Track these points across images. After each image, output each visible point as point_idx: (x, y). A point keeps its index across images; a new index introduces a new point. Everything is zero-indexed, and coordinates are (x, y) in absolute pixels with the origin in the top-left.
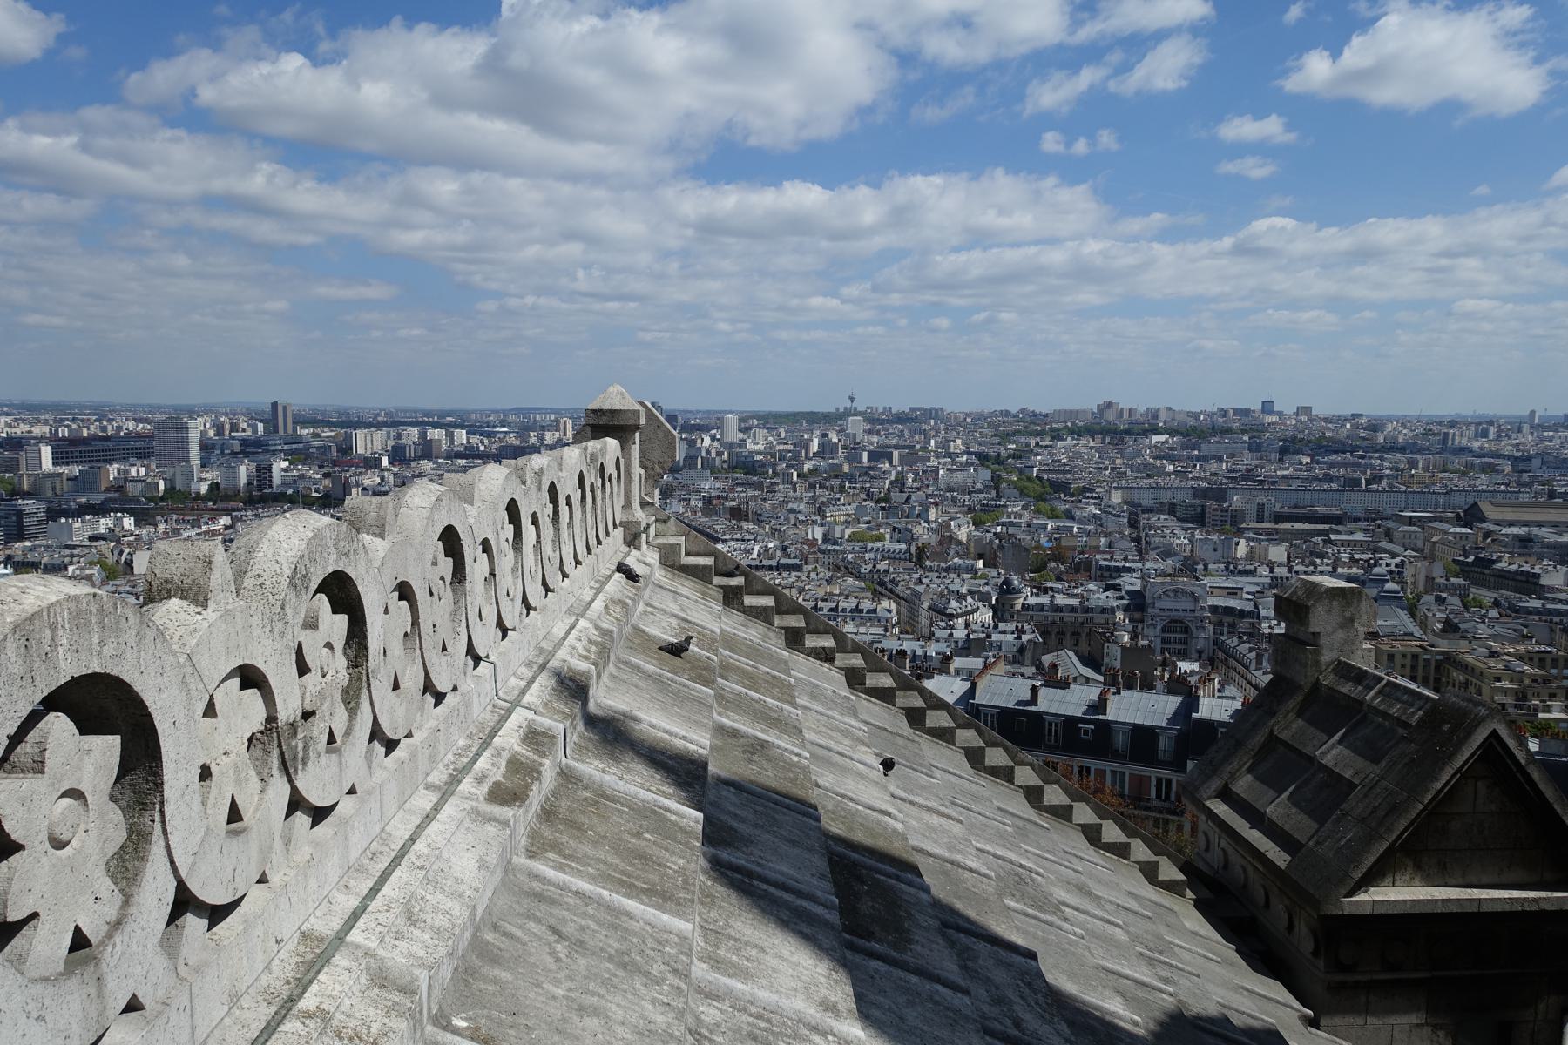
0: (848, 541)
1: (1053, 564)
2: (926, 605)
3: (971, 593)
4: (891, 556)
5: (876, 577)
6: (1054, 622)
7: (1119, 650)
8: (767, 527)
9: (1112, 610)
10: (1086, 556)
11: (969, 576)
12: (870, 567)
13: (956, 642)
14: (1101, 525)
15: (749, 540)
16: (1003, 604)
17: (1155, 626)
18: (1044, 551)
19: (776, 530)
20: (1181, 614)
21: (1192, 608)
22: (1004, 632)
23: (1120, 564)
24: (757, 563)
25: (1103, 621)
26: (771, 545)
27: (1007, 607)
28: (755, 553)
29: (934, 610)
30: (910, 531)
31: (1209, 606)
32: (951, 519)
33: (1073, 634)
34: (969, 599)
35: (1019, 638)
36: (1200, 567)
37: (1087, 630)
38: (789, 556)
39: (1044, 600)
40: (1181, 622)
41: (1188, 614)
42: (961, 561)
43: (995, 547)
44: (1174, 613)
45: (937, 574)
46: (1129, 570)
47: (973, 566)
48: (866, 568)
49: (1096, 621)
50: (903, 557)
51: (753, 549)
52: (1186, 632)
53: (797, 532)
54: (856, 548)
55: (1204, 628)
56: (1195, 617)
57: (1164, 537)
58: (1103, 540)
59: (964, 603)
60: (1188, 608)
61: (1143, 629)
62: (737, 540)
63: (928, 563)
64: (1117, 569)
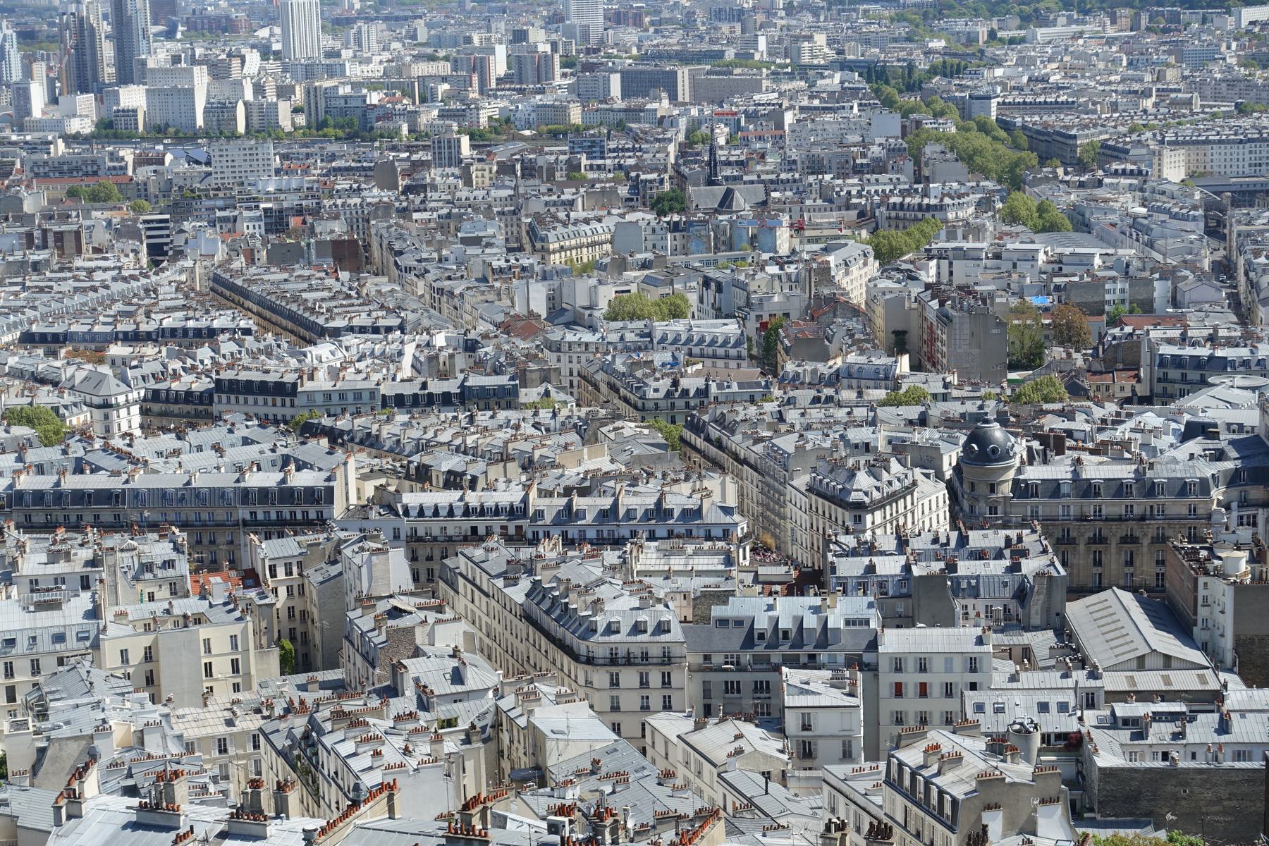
0: (612, 316)
1: (1057, 352)
2: (802, 481)
3: (899, 448)
5: (680, 403)
7: (1230, 591)
8: (421, 284)
10: (1128, 329)
11: (881, 394)
12: (665, 384)
13: (882, 585)
14: (1151, 245)
15: (389, 330)
19: (441, 291)
22: (979, 555)
23: (1204, 352)
24: (409, 390)
25: (1185, 511)
26: (440, 340)
27: (982, 489)
28: (407, 361)
29: (819, 494)
30: (743, 287)
32: (826, 250)
33: (1124, 540)
34: (895, 466)
35: (1015, 568)
37: (1152, 532)
38: (478, 366)
39: (1059, 470)
42: (863, 359)
43: (932, 317)
45: (813, 393)
46: (1222, 366)
50: (733, 352)
51: (400, 354)
53: (491, 297)
54: (630, 337)
59: (885, 476)
62: (362, 330)
64: (1197, 362)
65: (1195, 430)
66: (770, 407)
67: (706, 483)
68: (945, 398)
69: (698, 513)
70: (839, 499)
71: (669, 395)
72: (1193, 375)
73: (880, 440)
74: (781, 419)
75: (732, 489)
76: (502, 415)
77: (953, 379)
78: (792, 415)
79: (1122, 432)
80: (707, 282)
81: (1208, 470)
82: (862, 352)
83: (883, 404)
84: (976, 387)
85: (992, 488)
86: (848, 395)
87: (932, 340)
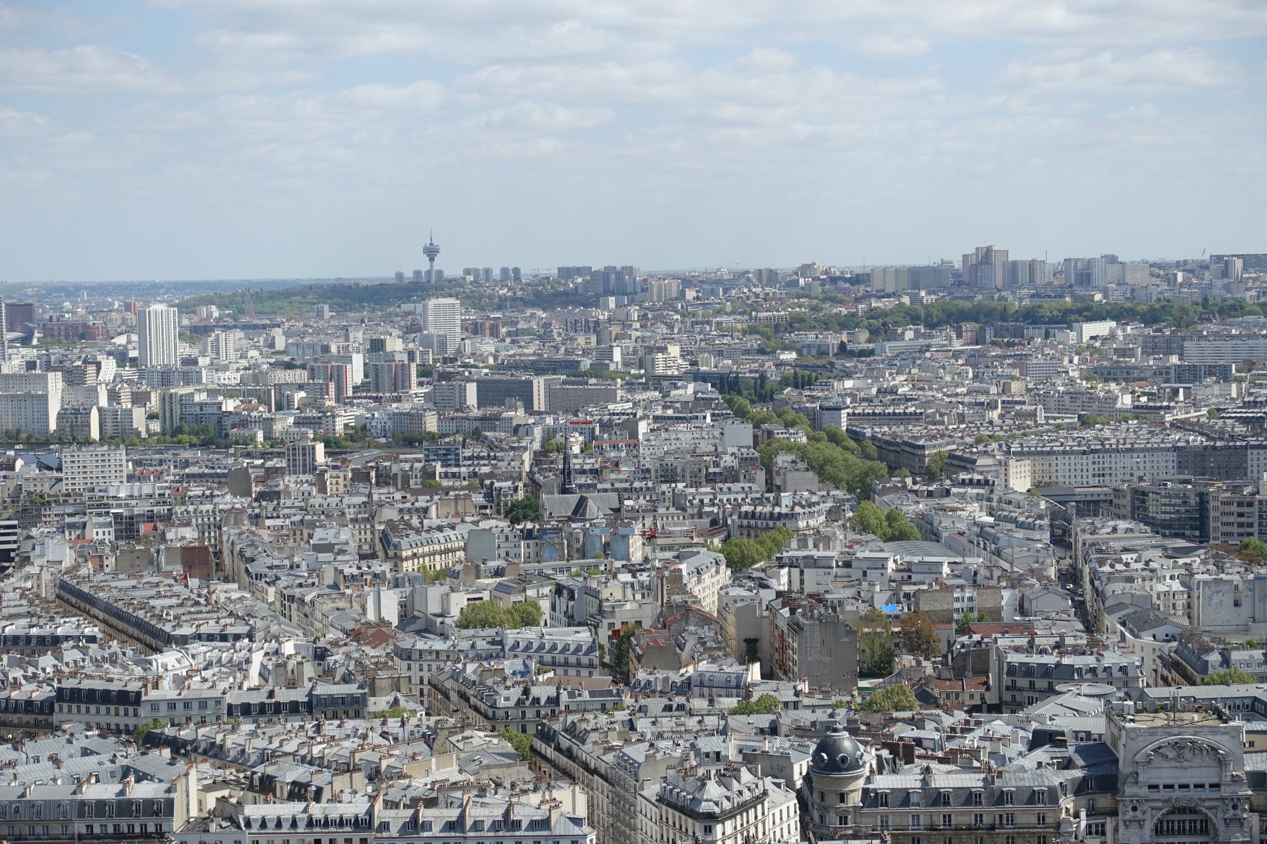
1: (907, 660)
2: (652, 790)
3: (749, 758)
4: (554, 660)
5: (530, 714)
6: (932, 828)
9: (1052, 796)
10: (976, 637)
11: (731, 702)
12: (516, 693)
14: (998, 553)
15: (237, 637)
16: (822, 796)
17: (1141, 823)
18: (886, 627)
19: (292, 598)
20: (1193, 794)
21: (1215, 781)
23: (1050, 660)
25: (1034, 820)
26: (288, 648)
27: (832, 799)
28: (255, 669)
29: (669, 805)
30: (595, 594)
31: (1247, 773)
34: (746, 776)
36: (1214, 658)
38: (328, 674)
39: (908, 779)
40: (1193, 811)
41: (1207, 793)
43: (783, 625)
44: (1178, 793)
45: (665, 701)
46: (1068, 674)
47: (739, 677)
48: (507, 697)
49: (1021, 819)
50: (585, 660)
51: (248, 661)
52: (1204, 831)
53: (341, 604)
54: (481, 644)
55: (1241, 822)
56: (1223, 799)
57: (1130, 580)
58: (1006, 594)
60: (1207, 782)
61: (1116, 830)
62: (210, 637)
63: (642, 675)
64: (1046, 671)
65: (1040, 739)
66: (621, 716)
67: (556, 794)
68: (796, 705)
69: (545, 824)
70: (689, 810)
71: (520, 703)
72: (1041, 684)
73: (731, 750)
74: (632, 728)
75: (582, 799)
76: (350, 724)
77: (804, 687)
78: (642, 724)
79: (971, 740)
80: (559, 590)
81: (1056, 778)
82: (714, 660)
83: (734, 712)
84: (826, 694)
85: (842, 797)
86: (699, 704)
87: (784, 648)
